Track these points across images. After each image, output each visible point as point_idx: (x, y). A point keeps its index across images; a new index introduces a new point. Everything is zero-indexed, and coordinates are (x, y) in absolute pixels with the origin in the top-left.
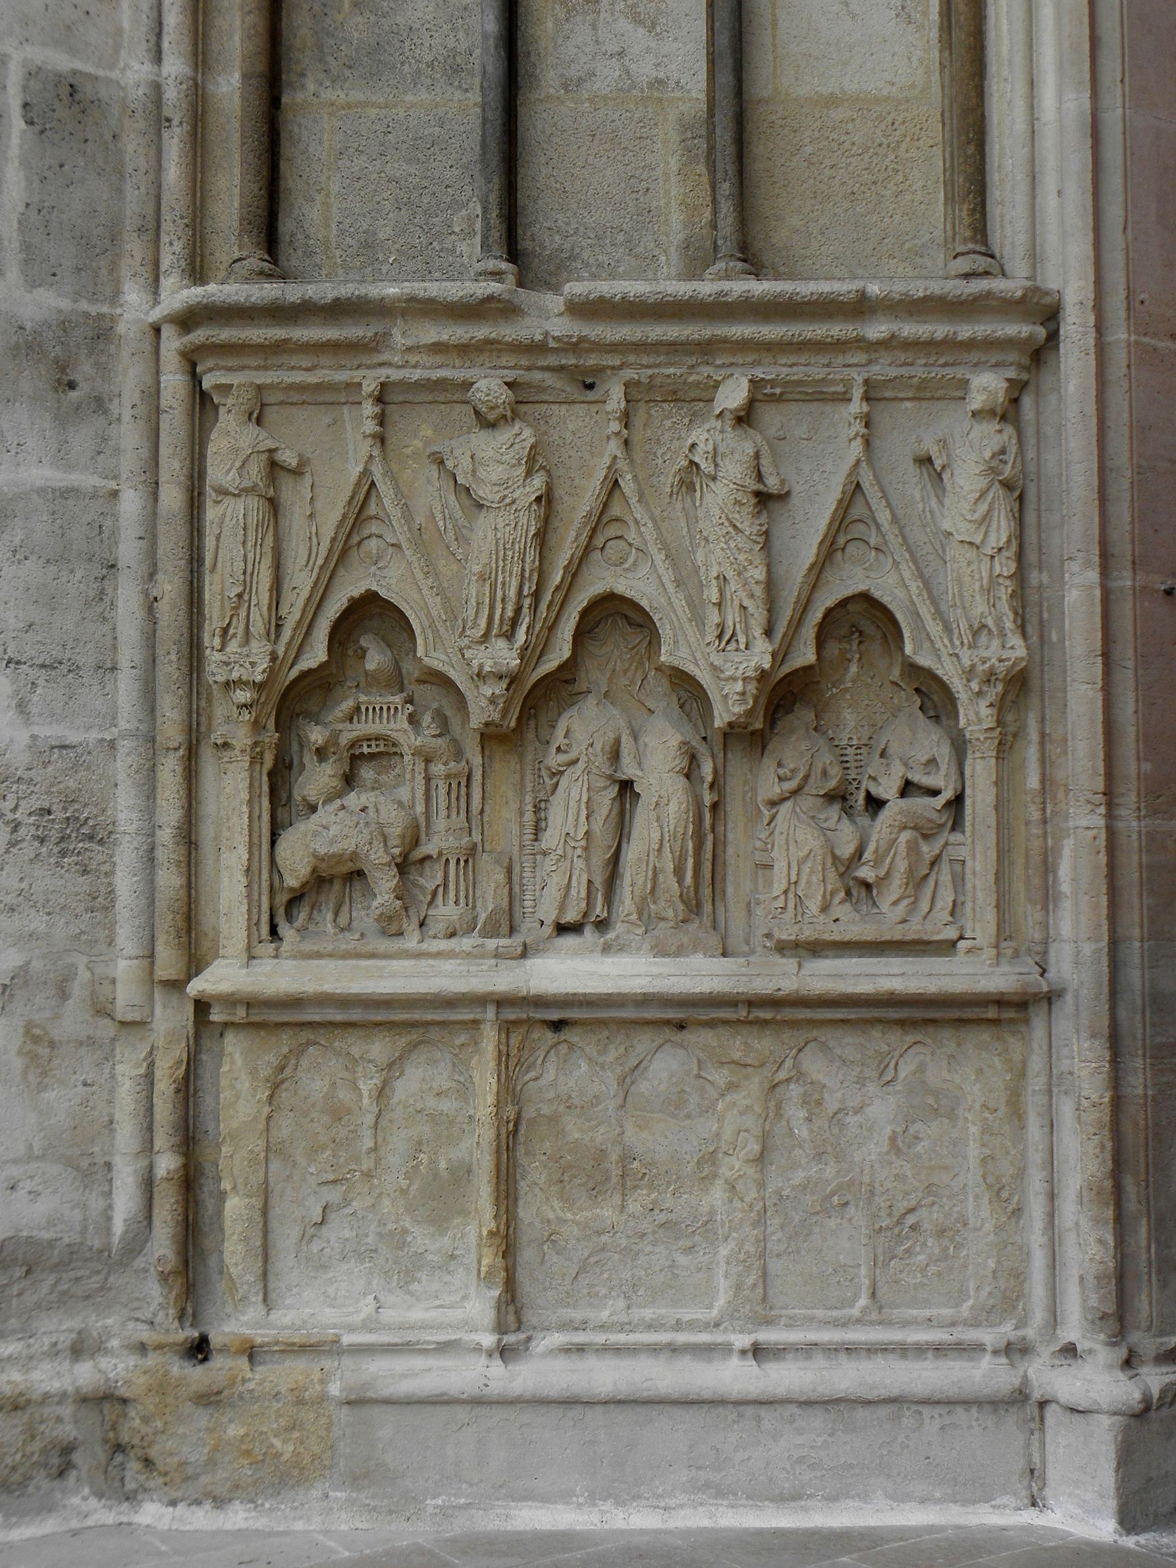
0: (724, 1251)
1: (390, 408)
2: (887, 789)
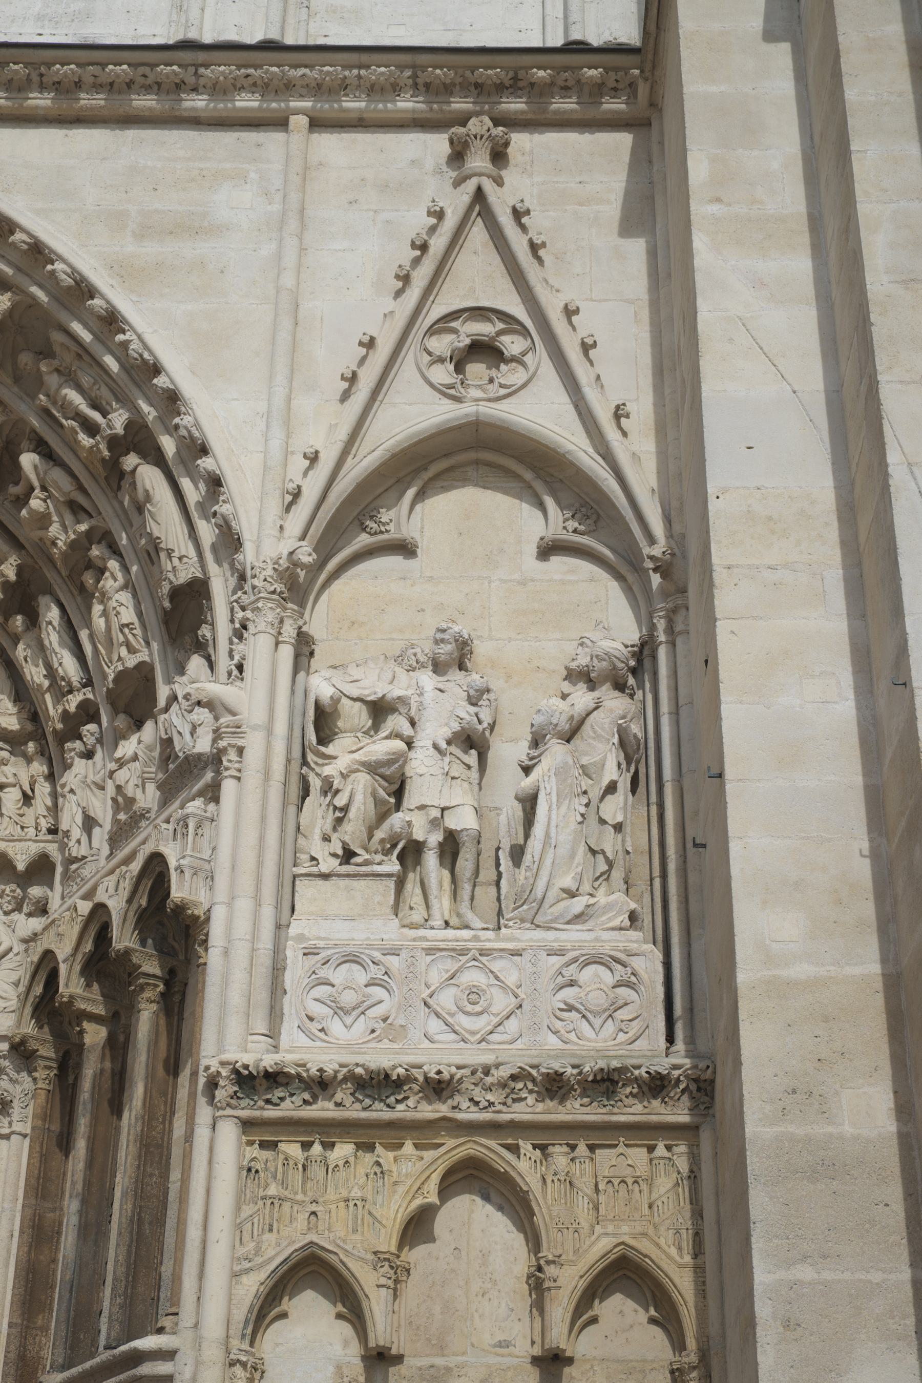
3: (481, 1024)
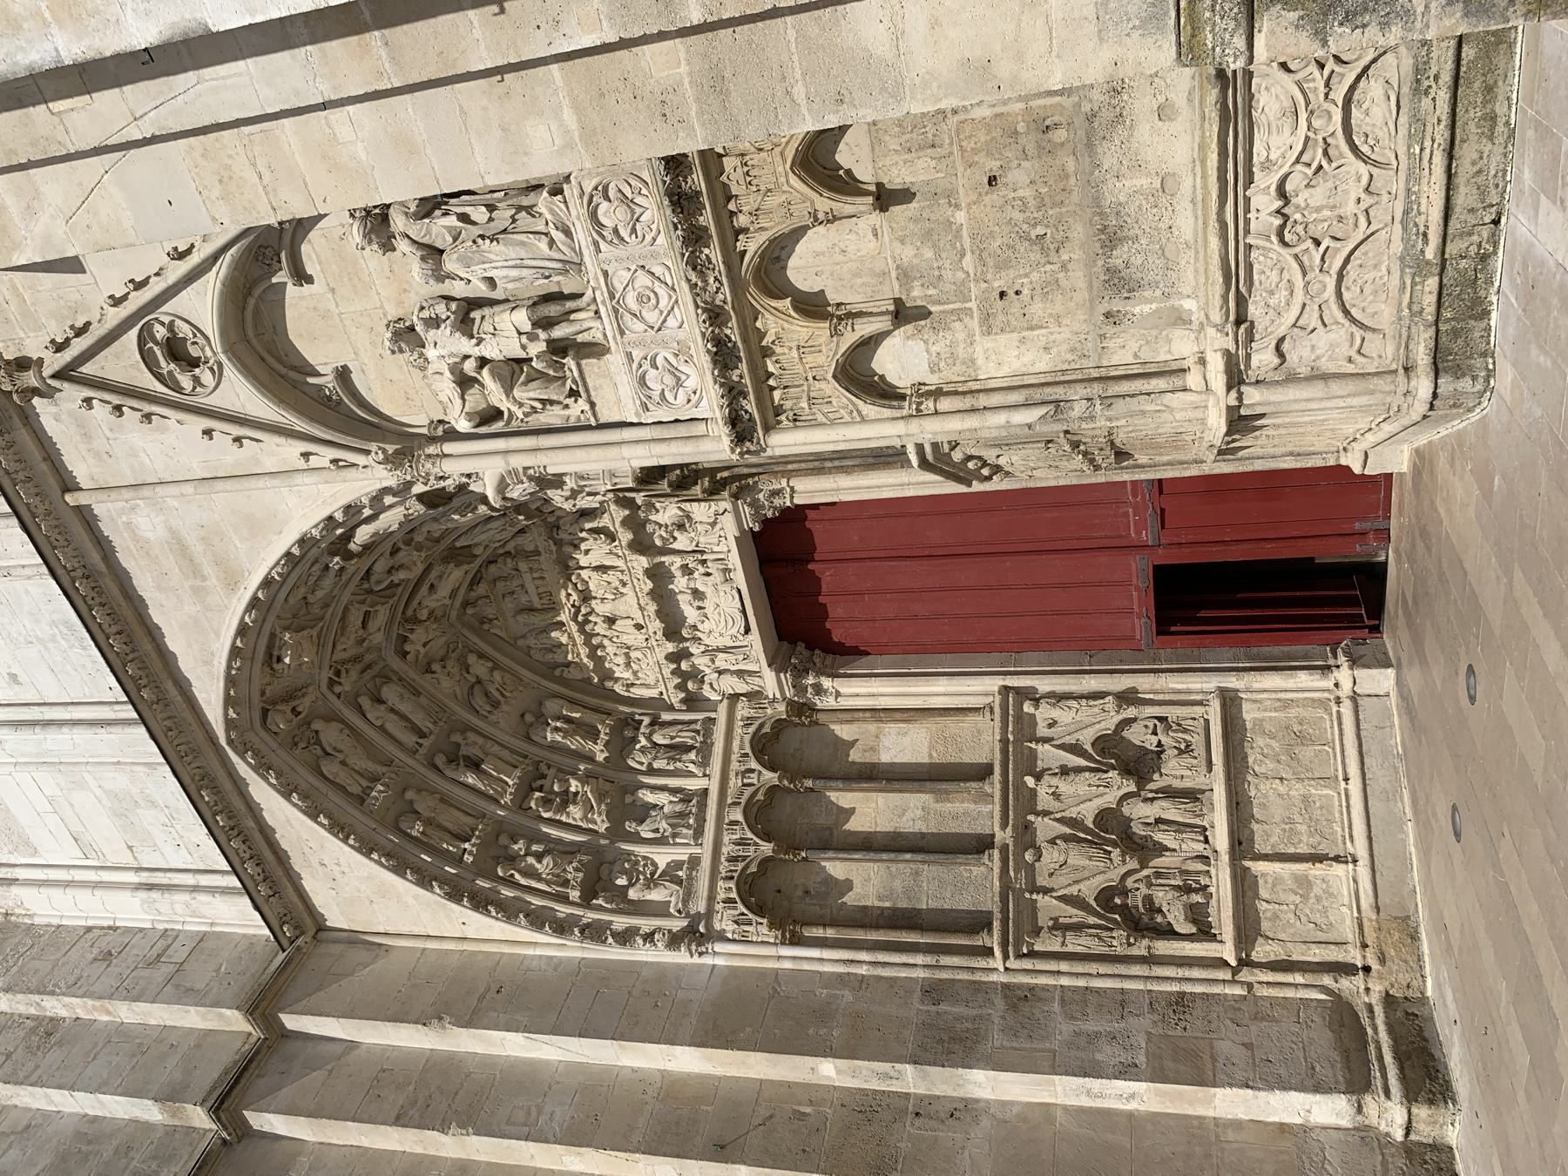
0: (1313, 791)
2: (1154, 740)
3: (661, 291)
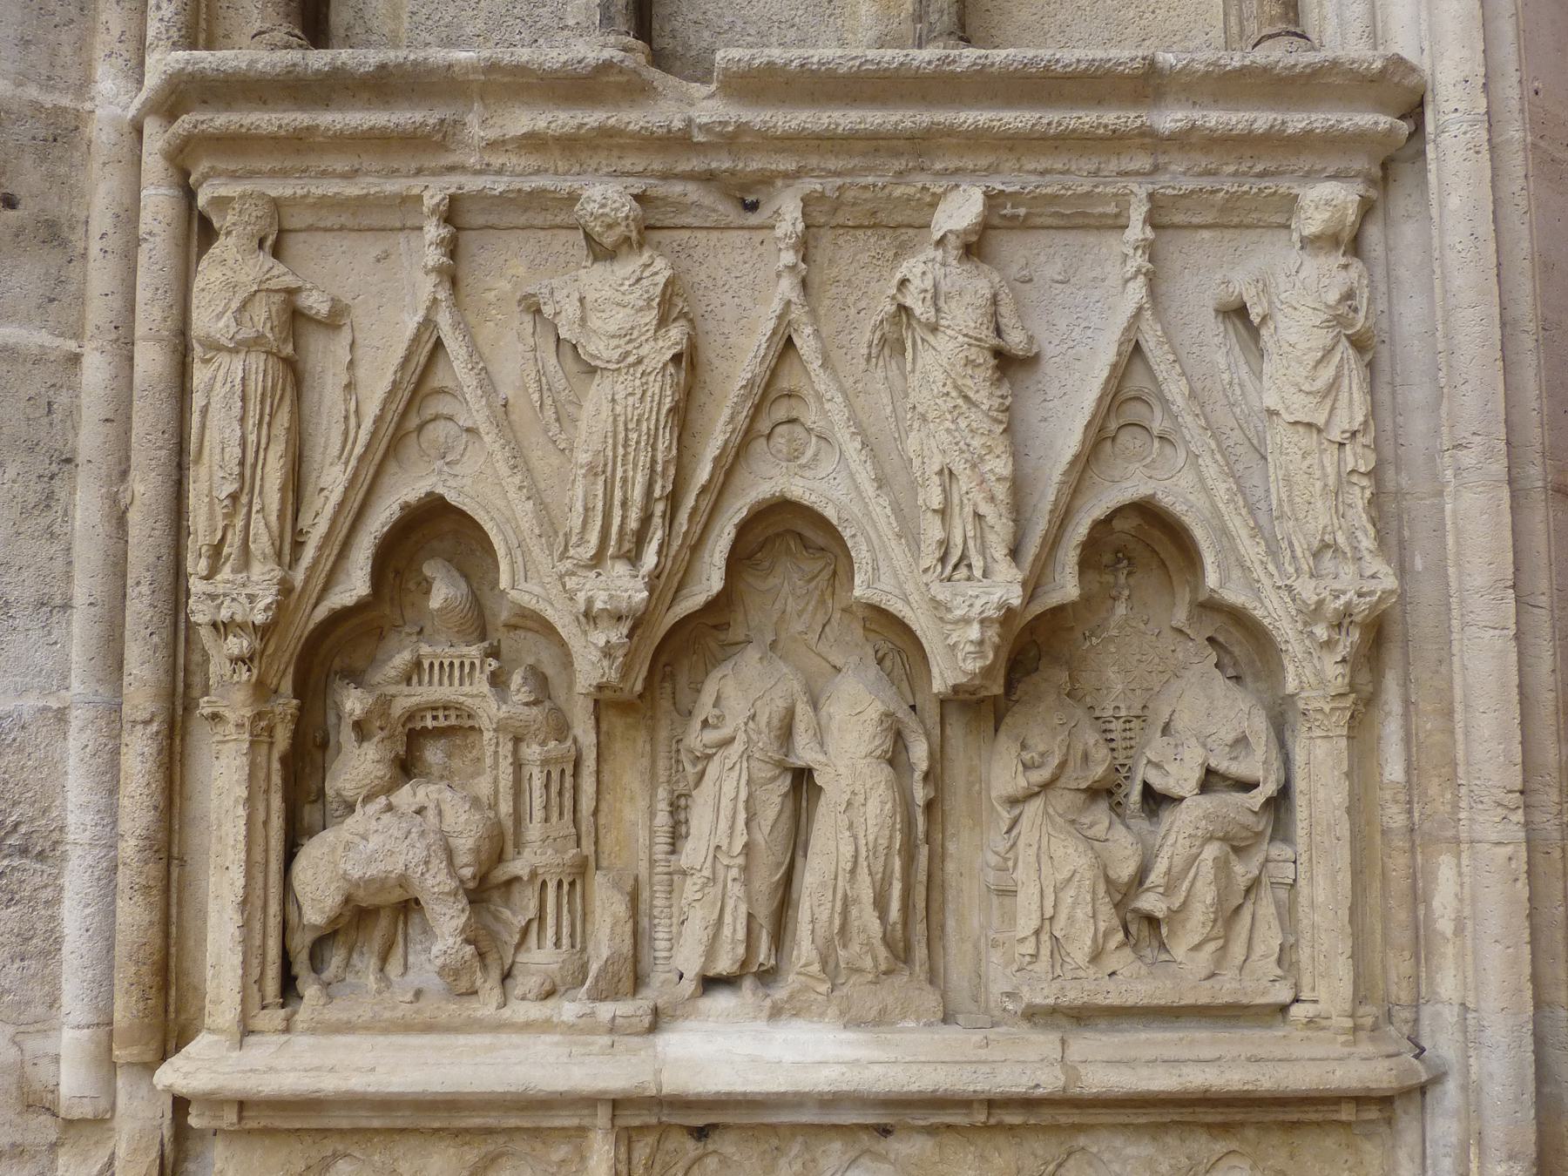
1: (465, 236)
2: (1180, 777)
